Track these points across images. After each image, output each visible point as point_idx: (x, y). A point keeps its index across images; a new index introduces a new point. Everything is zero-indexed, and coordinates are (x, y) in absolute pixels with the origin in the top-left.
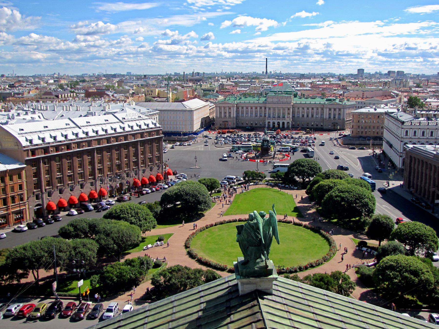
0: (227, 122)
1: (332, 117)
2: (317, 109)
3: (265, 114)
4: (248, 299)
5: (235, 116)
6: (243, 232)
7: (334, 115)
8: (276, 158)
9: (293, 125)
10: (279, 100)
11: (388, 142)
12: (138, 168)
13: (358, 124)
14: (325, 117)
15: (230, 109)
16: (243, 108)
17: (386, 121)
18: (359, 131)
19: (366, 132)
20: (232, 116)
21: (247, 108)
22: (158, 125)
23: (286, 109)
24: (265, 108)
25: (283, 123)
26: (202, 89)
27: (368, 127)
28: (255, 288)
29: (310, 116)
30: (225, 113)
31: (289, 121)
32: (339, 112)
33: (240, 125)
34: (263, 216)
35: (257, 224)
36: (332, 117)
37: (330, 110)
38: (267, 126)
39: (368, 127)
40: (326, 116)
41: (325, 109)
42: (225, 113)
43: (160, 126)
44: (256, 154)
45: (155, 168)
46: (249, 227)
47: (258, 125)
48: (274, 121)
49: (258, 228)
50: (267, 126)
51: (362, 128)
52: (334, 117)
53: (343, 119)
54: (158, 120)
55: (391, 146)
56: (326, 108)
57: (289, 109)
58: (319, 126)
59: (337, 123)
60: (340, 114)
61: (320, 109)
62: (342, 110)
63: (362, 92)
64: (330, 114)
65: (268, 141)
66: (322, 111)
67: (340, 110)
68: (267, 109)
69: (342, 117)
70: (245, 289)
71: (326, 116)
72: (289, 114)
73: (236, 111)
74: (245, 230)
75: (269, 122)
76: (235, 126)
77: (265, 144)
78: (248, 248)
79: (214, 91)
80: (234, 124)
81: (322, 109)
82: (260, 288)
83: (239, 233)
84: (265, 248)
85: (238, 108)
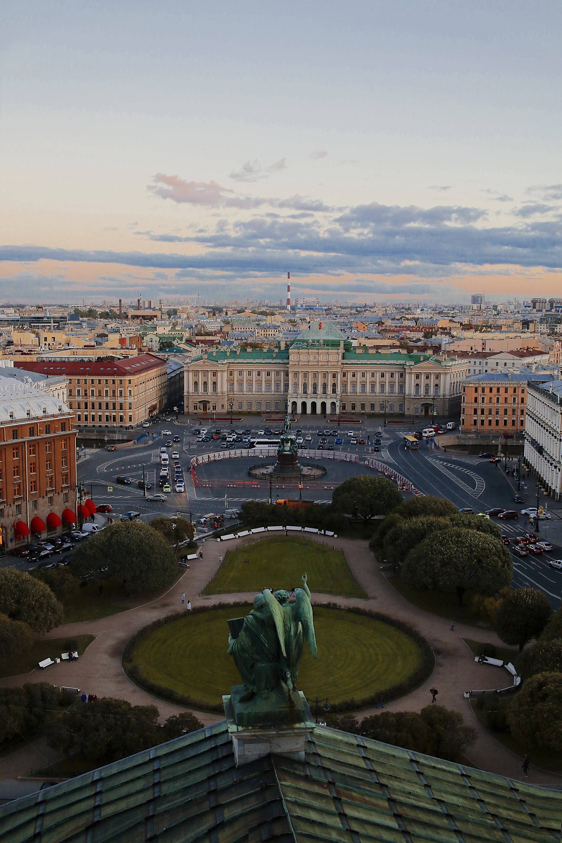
0: (209, 402)
4: (253, 775)
5: (225, 389)
6: (242, 633)
7: (427, 386)
9: (344, 407)
10: (315, 358)
11: (534, 443)
12: (24, 499)
13: (475, 405)
15: (215, 374)
17: (529, 400)
18: (475, 421)
19: (490, 421)
20: (219, 390)
22: (66, 409)
23: (330, 376)
24: (287, 375)
25: (324, 405)
27: (494, 413)
28: (269, 751)
29: (378, 389)
30: (205, 383)
31: (334, 401)
32: (437, 382)
33: (235, 408)
34: (282, 601)
35: (271, 619)
36: (422, 391)
37: (417, 377)
38: (290, 410)
39: (494, 413)
41: (407, 376)
42: (205, 383)
43: (71, 411)
45: (59, 499)
46: (254, 622)
48: (305, 400)
49: (274, 626)
50: (290, 410)
51: (482, 413)
52: (427, 392)
54: (65, 399)
55: (540, 450)
56: (410, 373)
57: (334, 376)
58: (396, 410)
59: (431, 405)
60: (437, 385)
61: (397, 376)
62: (442, 377)
63: (481, 342)
64: (417, 385)
66: (401, 379)
67: (437, 377)
68: (290, 375)
69: (442, 392)
70: (247, 753)
71: (410, 389)
72: (334, 385)
73: (227, 381)
74: (247, 629)
75: (294, 403)
77: (287, 448)
78: (253, 666)
79: (181, 339)
82: (278, 750)
83: (235, 636)
84: (289, 666)
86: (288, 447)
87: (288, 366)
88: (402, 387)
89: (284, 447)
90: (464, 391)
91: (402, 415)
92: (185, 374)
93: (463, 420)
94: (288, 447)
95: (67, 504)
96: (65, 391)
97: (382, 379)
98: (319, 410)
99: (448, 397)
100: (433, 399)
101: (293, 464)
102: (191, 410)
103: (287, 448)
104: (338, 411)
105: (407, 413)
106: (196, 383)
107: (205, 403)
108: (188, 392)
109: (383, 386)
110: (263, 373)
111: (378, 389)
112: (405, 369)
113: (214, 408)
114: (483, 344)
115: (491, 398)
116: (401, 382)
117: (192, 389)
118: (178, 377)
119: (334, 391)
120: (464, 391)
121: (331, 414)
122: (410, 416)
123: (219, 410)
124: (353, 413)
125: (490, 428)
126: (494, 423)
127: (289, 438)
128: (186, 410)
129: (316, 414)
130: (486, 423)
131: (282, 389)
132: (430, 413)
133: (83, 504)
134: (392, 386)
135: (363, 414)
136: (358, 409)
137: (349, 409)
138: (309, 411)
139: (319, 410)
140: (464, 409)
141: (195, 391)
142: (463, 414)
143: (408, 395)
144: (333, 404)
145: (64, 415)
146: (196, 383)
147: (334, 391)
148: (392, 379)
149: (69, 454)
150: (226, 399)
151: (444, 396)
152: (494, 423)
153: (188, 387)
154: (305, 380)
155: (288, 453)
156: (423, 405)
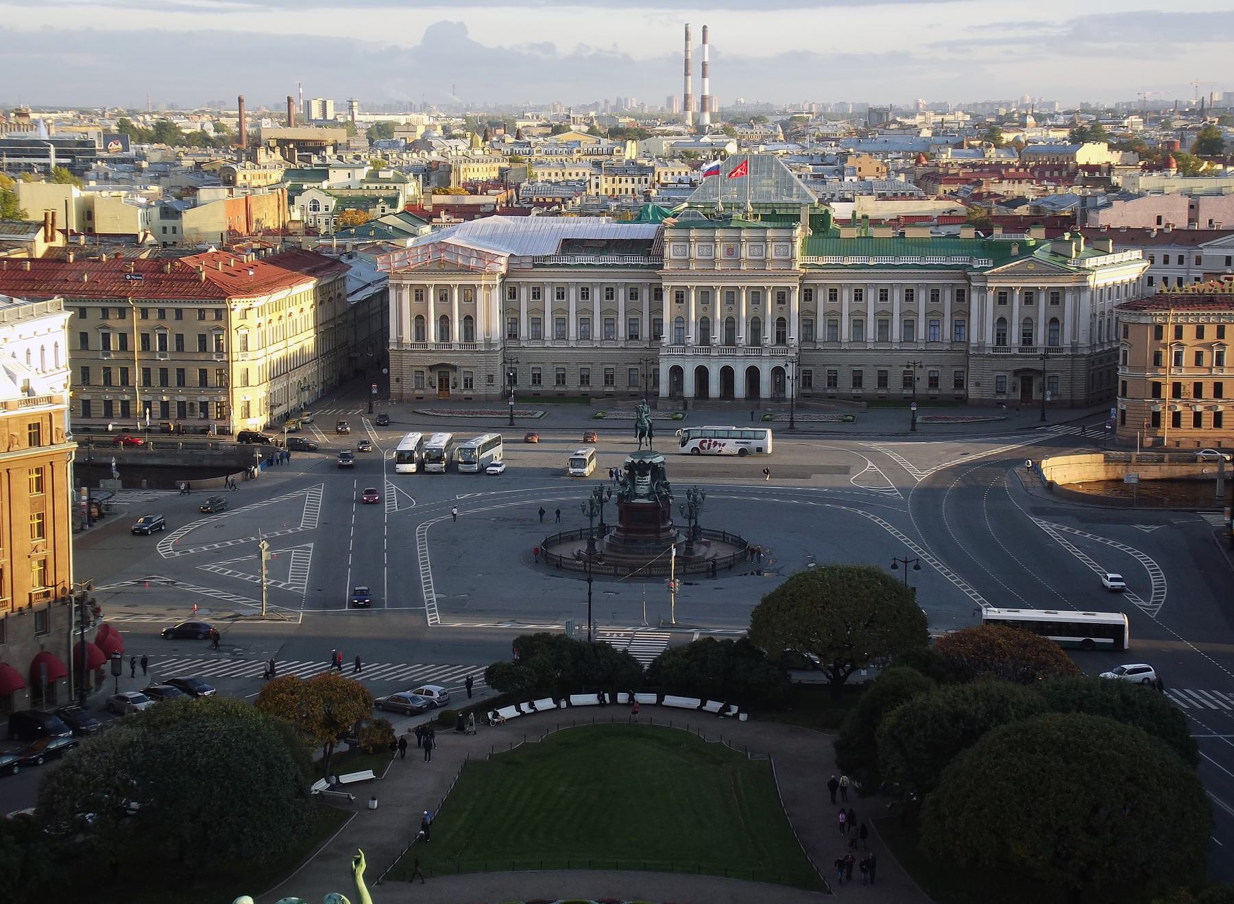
0: (454, 368)
1: (1015, 337)
2: (935, 296)
3: (657, 324)
8: (701, 560)
9: (806, 379)
14: (974, 339)
16: (537, 294)
21: (561, 295)
24: (658, 294)
25: (753, 374)
26: (328, 192)
29: (896, 331)
30: (444, 321)
32: (1054, 312)
33: (525, 383)
36: (1015, 337)
38: (664, 390)
40: (981, 331)
41: (974, 297)
42: (444, 321)
44: (591, 545)
47: (621, 385)
48: (703, 362)
50: (664, 390)
52: (1027, 338)
53: (1074, 347)
58: (946, 386)
59: (1041, 373)
61: (947, 297)
62: (1069, 298)
63: (1186, 201)
64: (1002, 321)
65: (657, 472)
66: (960, 306)
68: (667, 298)
69: (1067, 339)
71: (981, 331)
72: (781, 323)
73: (505, 311)
75: (677, 372)
76: (497, 390)
77: (643, 489)
79: (393, 201)
80: (490, 378)
81: (961, 295)
85: (513, 295)
86: (645, 484)
87: (659, 272)
88: (961, 323)
89: (634, 485)
90: (1126, 336)
91: (960, 402)
92: (392, 294)
93: (1123, 412)
94: (645, 484)
95: (43, 639)
96: (63, 339)
97: (909, 306)
98: (740, 388)
99: (1087, 352)
100: (1043, 357)
101: (657, 531)
102: (408, 386)
103: (643, 489)
104: (790, 391)
105: (973, 392)
106: (420, 321)
107: (443, 371)
108: (399, 342)
109: (909, 326)
110: (597, 292)
111: (896, 331)
112: (969, 278)
113: (469, 384)
114: (1191, 207)
115: (1199, 355)
116: (958, 313)
117: (408, 336)
118: (377, 302)
119: (781, 338)
120: (1126, 336)
121: (772, 399)
122: (982, 404)
123: (480, 388)
124: (832, 397)
125: (1197, 433)
126: (1207, 420)
127: (647, 461)
128: (394, 388)
129: (733, 398)
130: (1187, 419)
131: (646, 332)
132: (1036, 395)
133: (91, 639)
134: (934, 323)
135: (857, 398)
136: (845, 385)
137: (820, 383)
138: (714, 389)
139: (740, 388)
140: (1124, 383)
141: (417, 339)
142: (1124, 394)
143: (978, 349)
144: (778, 372)
145: (36, 402)
146: (420, 321)
147: (781, 338)
148: (934, 306)
149: (50, 507)
150: (500, 361)
151: (1074, 347)
152: (1207, 420)
153: (401, 329)
154: (705, 309)
155: (645, 501)
156: (1016, 373)
